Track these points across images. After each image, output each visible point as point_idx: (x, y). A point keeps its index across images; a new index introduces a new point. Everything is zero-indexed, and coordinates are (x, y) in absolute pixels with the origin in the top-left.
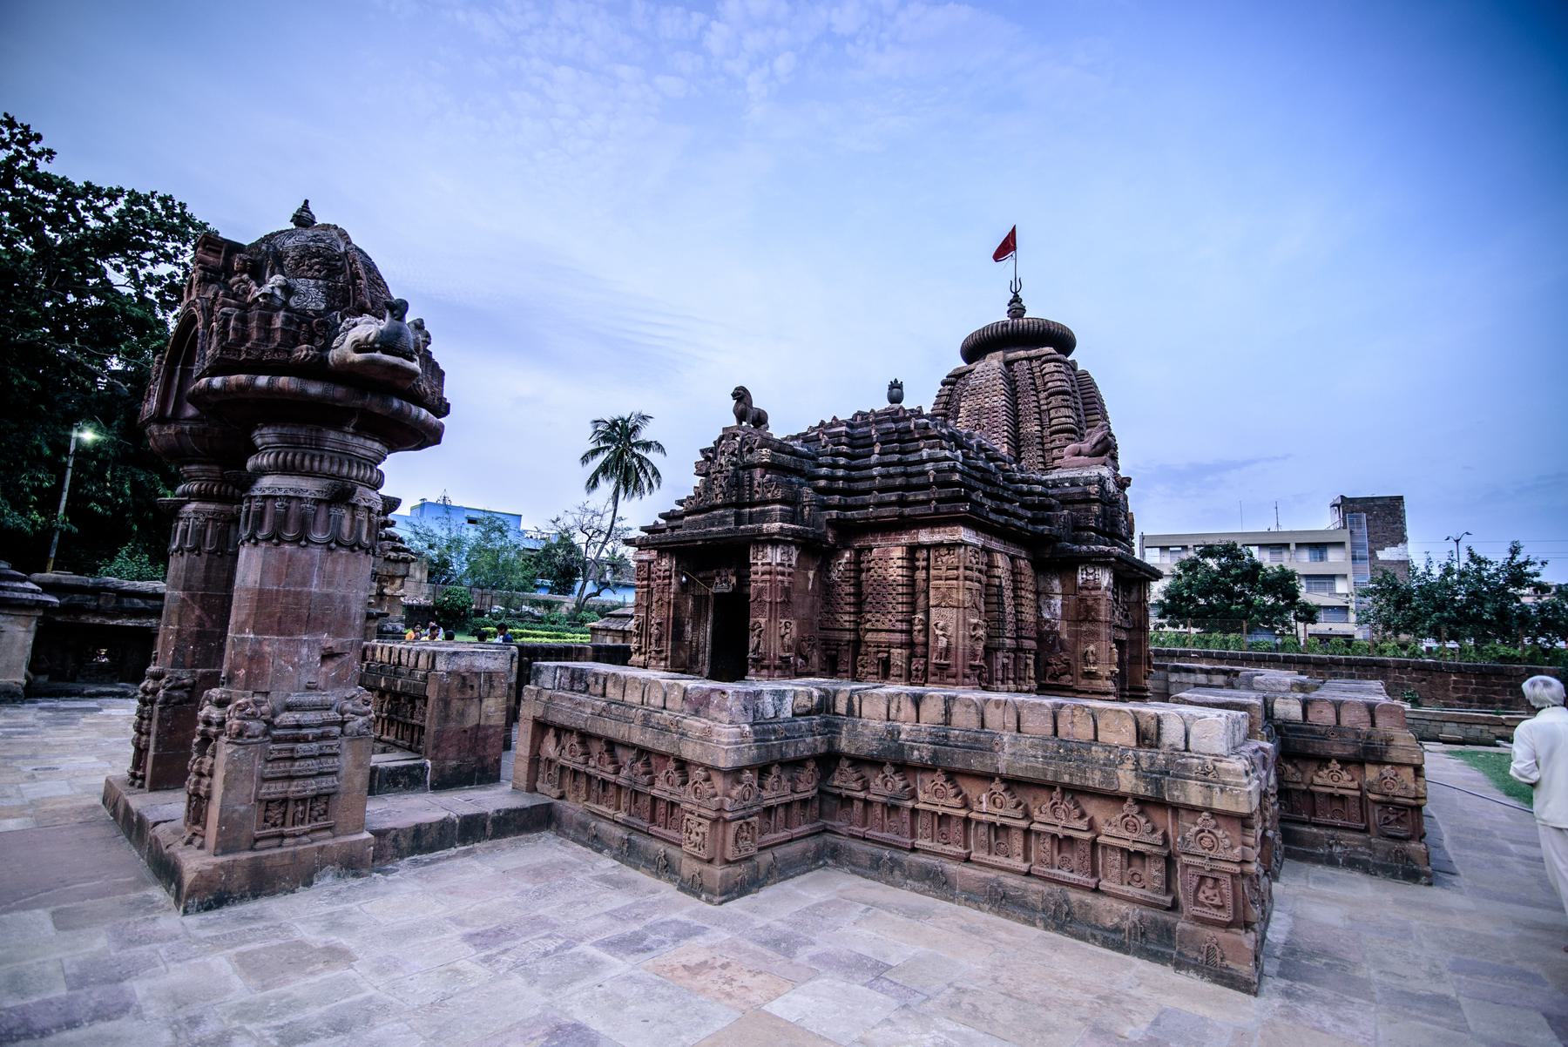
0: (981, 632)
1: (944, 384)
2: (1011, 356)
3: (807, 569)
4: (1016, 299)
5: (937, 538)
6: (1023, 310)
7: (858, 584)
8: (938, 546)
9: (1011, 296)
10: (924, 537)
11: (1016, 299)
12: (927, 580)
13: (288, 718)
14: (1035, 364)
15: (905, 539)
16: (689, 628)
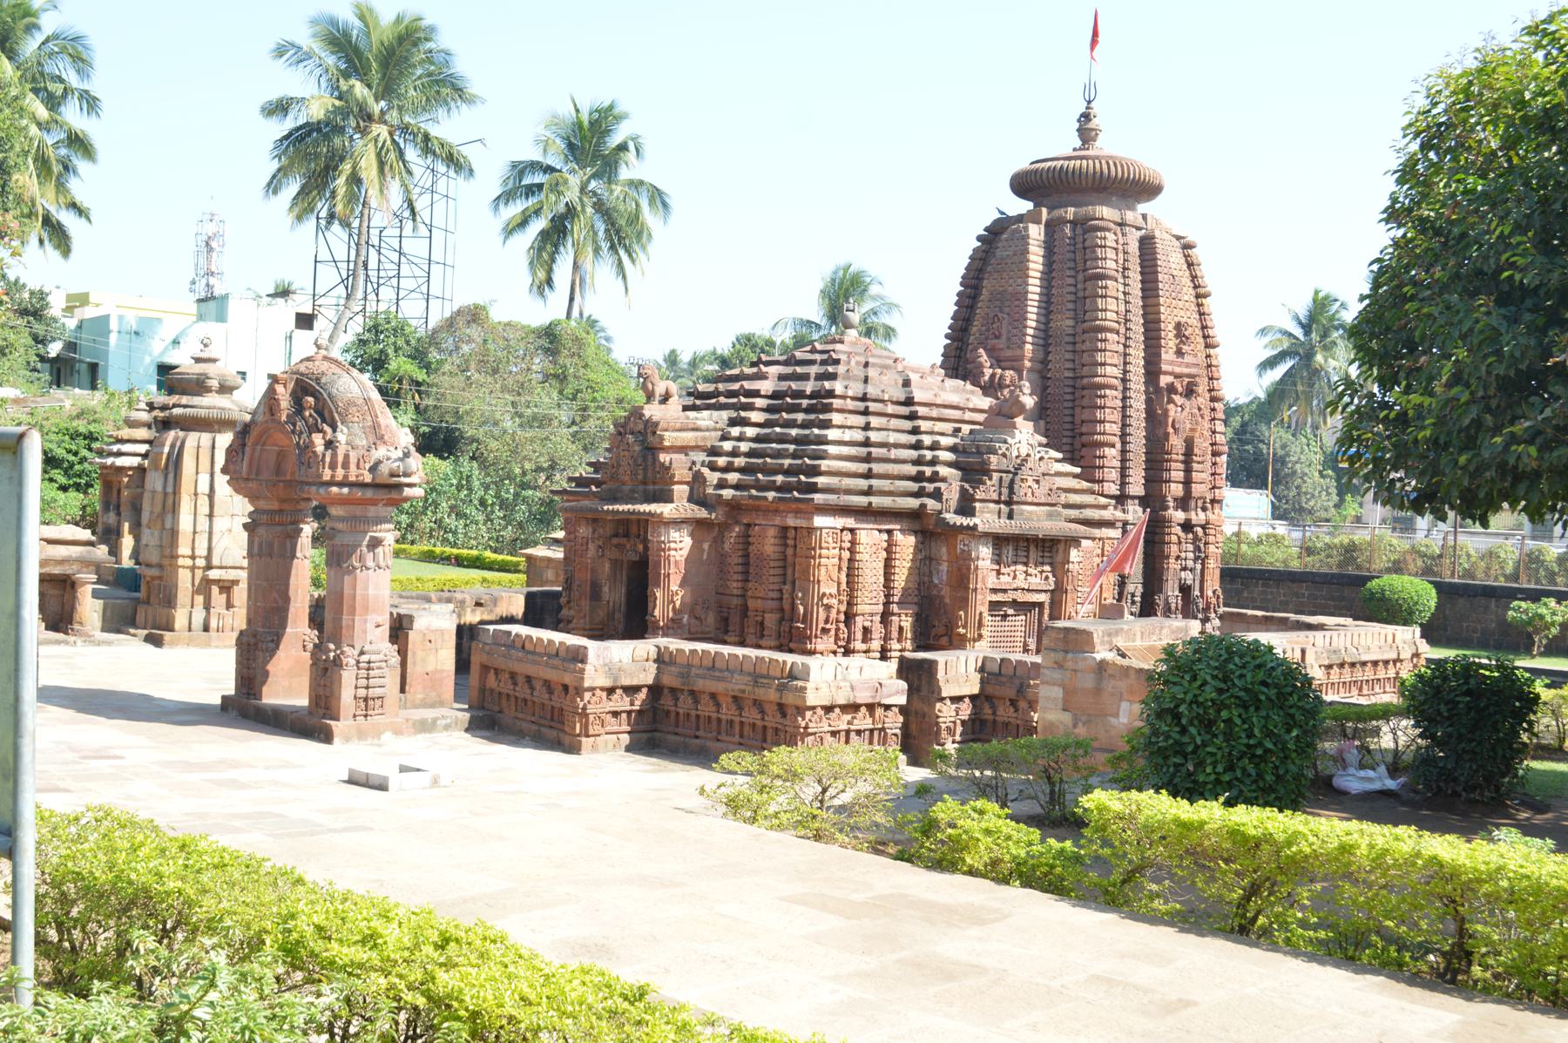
0: (834, 602)
1: (979, 238)
3: (701, 542)
7: (746, 556)
11: (1086, 117)
13: (365, 658)
15: (778, 521)
16: (606, 589)
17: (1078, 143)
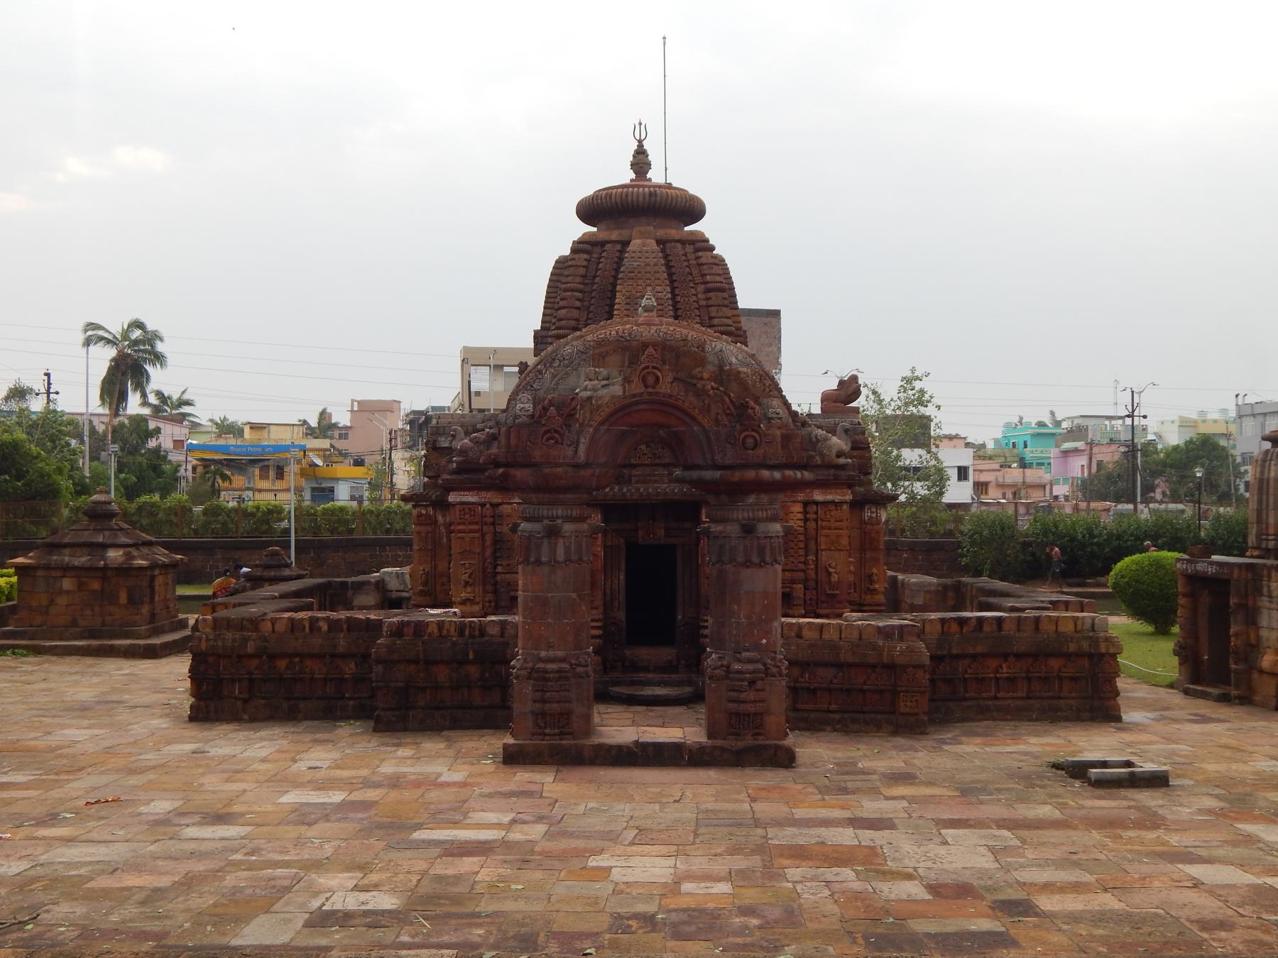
2: (661, 233)
4: (641, 153)
5: (830, 497)
6: (648, 165)
8: (832, 502)
9: (635, 146)
10: (818, 496)
11: (641, 153)
12: (817, 529)
14: (689, 249)
15: (801, 496)
17: (633, 176)
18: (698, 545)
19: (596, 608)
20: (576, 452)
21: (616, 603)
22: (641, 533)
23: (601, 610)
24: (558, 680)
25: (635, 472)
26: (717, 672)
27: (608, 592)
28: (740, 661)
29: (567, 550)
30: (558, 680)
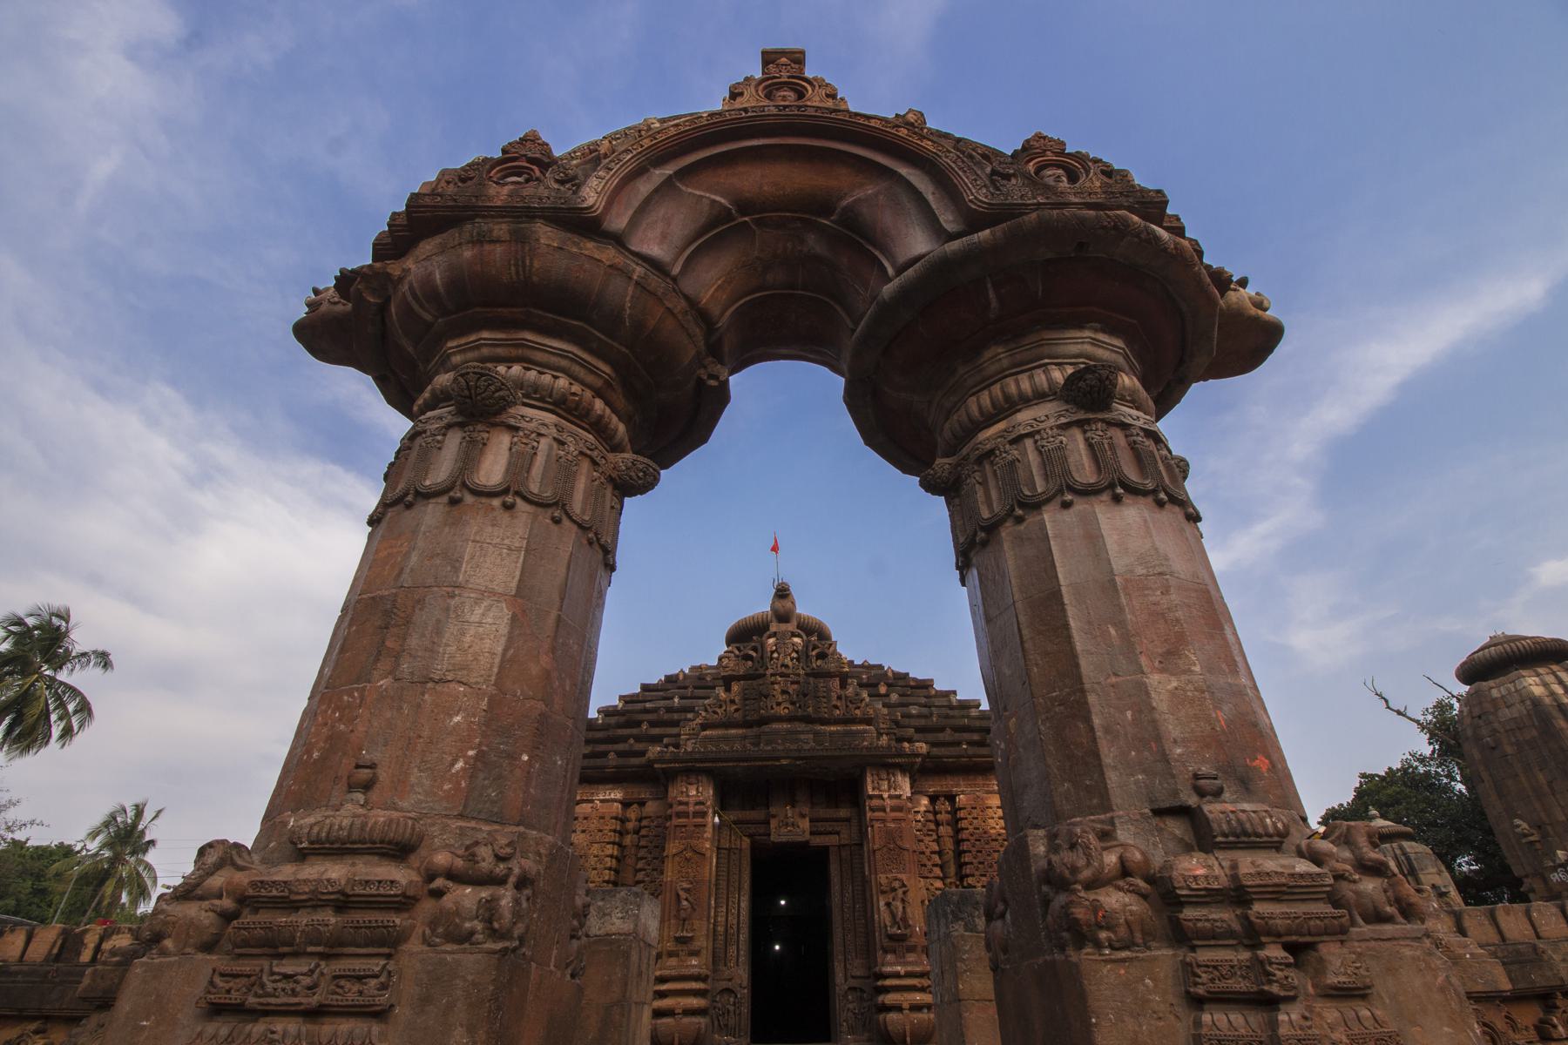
18: (861, 845)
19: (695, 953)
20: (575, 193)
21: (732, 950)
22: (774, 823)
23: (706, 956)
24: (332, 947)
25: (766, 728)
26: (1113, 899)
27: (720, 929)
28: (1204, 838)
29: (520, 464)
30: (332, 947)
